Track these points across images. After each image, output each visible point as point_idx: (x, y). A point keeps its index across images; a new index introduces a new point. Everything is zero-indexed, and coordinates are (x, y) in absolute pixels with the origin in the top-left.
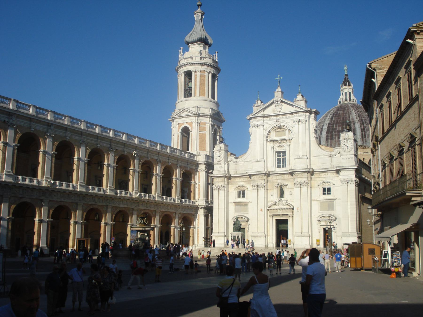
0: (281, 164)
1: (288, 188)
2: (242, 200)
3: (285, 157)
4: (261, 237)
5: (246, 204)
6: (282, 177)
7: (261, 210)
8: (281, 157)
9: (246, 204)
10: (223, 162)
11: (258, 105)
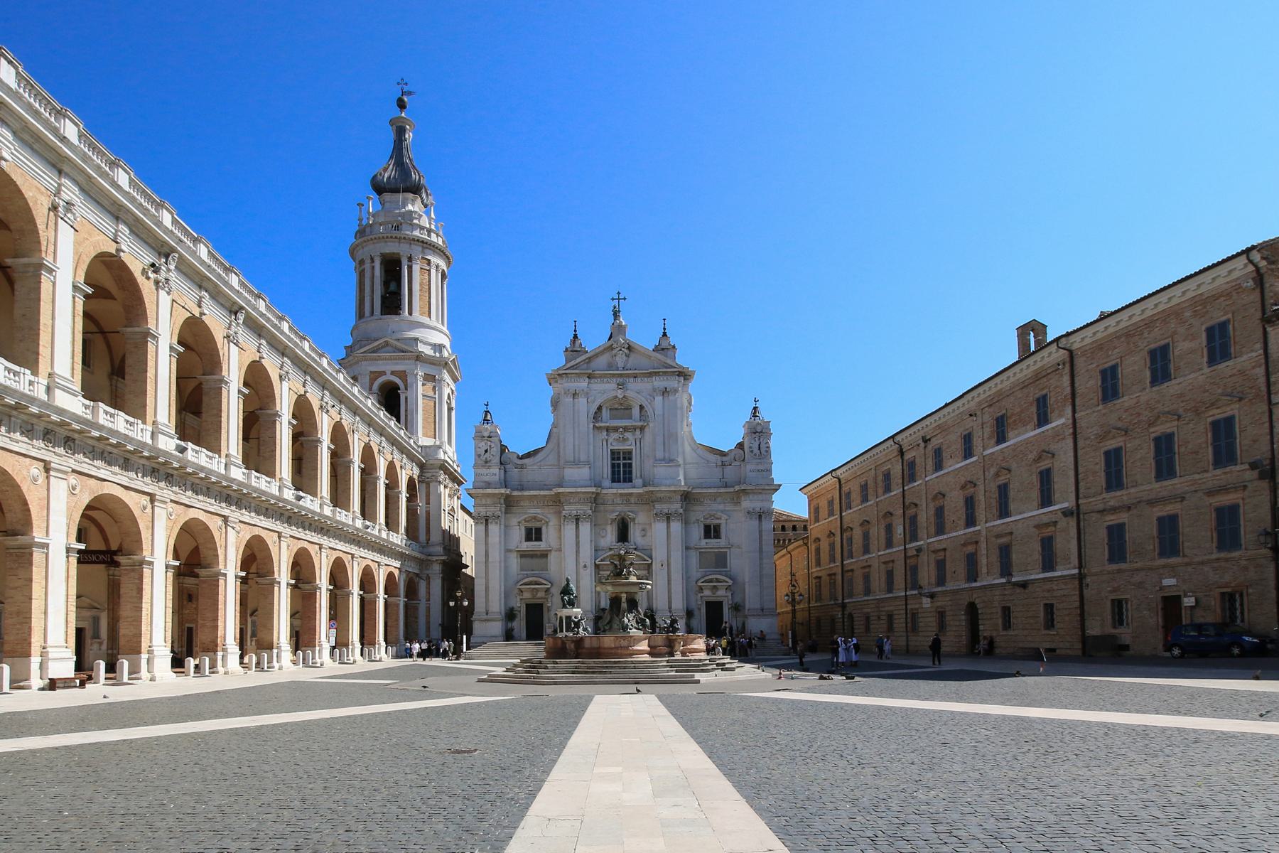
0: (620, 475)
2: (533, 546)
3: (630, 461)
5: (544, 555)
7: (585, 566)
8: (622, 462)
9: (544, 555)
11: (575, 349)
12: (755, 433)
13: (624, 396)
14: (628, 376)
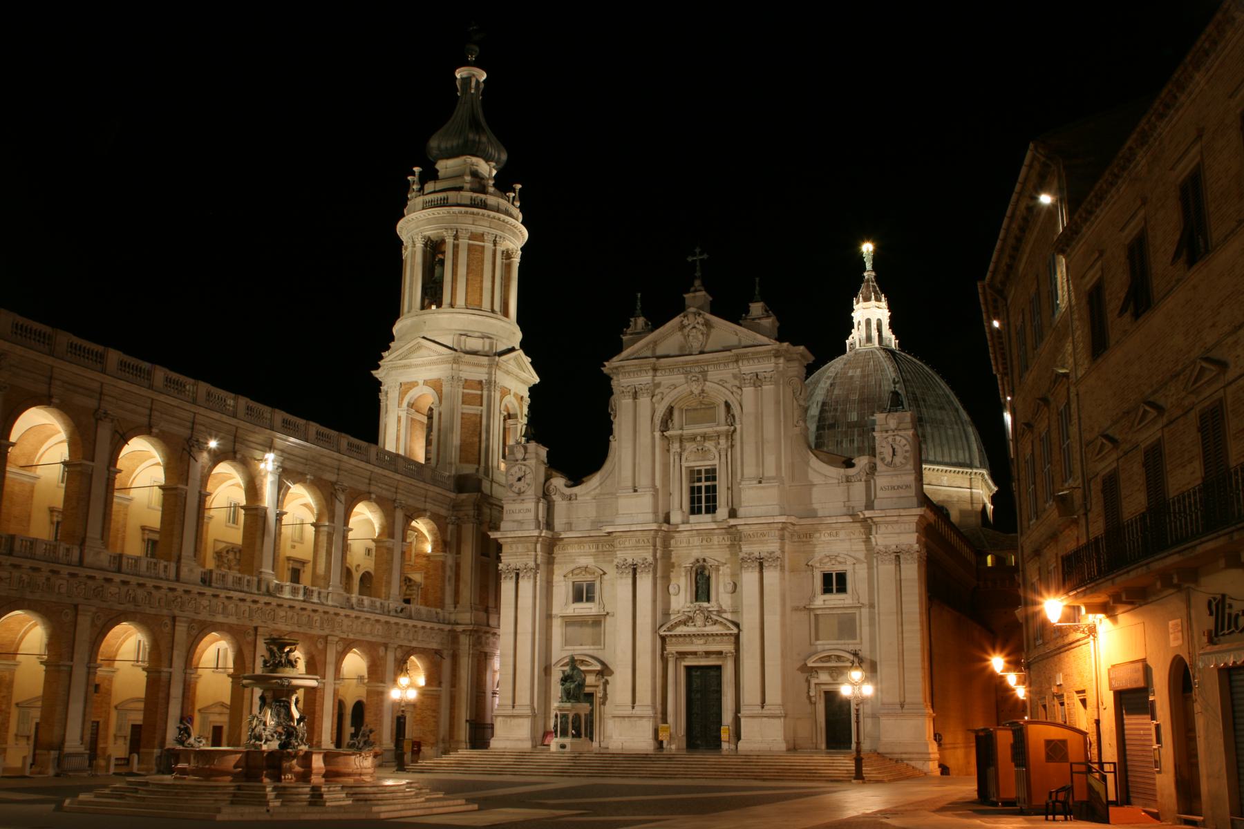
1: (721, 572)
3: (713, 483)
4: (641, 717)
5: (597, 622)
6: (704, 542)
8: (703, 484)
9: (597, 622)
10: (531, 493)
12: (887, 431)
13: (703, 391)
14: (708, 363)
